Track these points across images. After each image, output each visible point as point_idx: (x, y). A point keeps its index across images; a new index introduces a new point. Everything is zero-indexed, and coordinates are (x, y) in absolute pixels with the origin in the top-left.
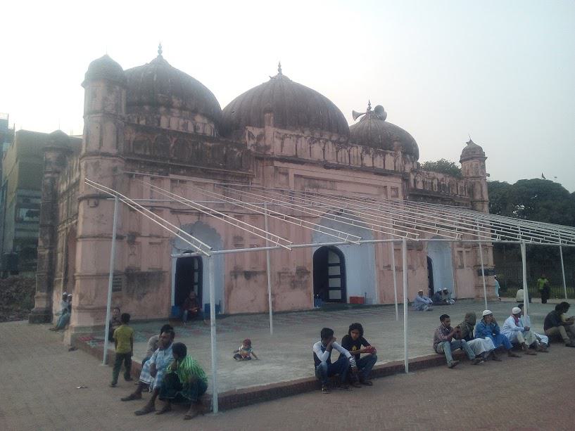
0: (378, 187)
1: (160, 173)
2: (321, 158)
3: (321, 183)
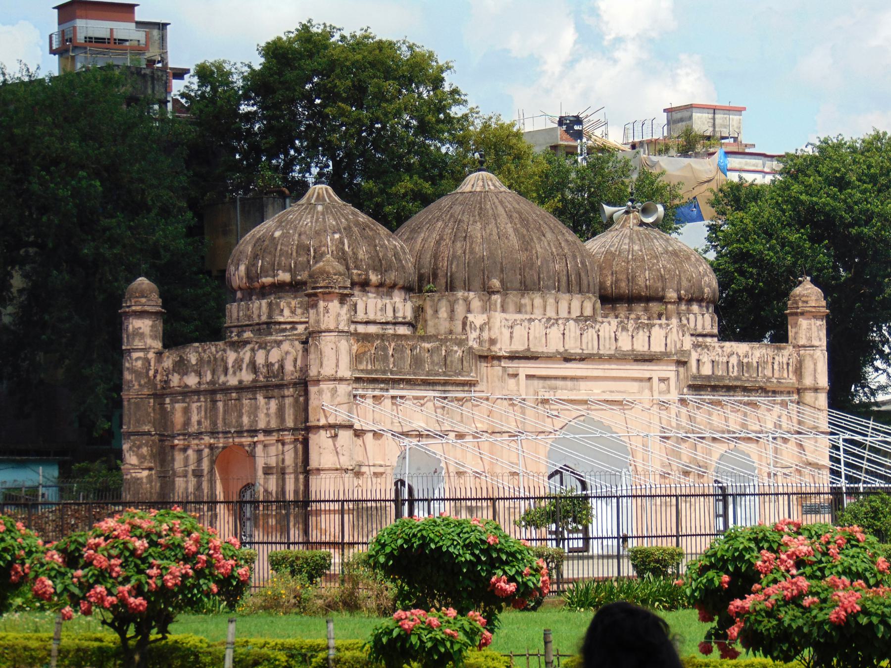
0: (641, 380)
1: (381, 389)
2: (561, 350)
3: (560, 383)
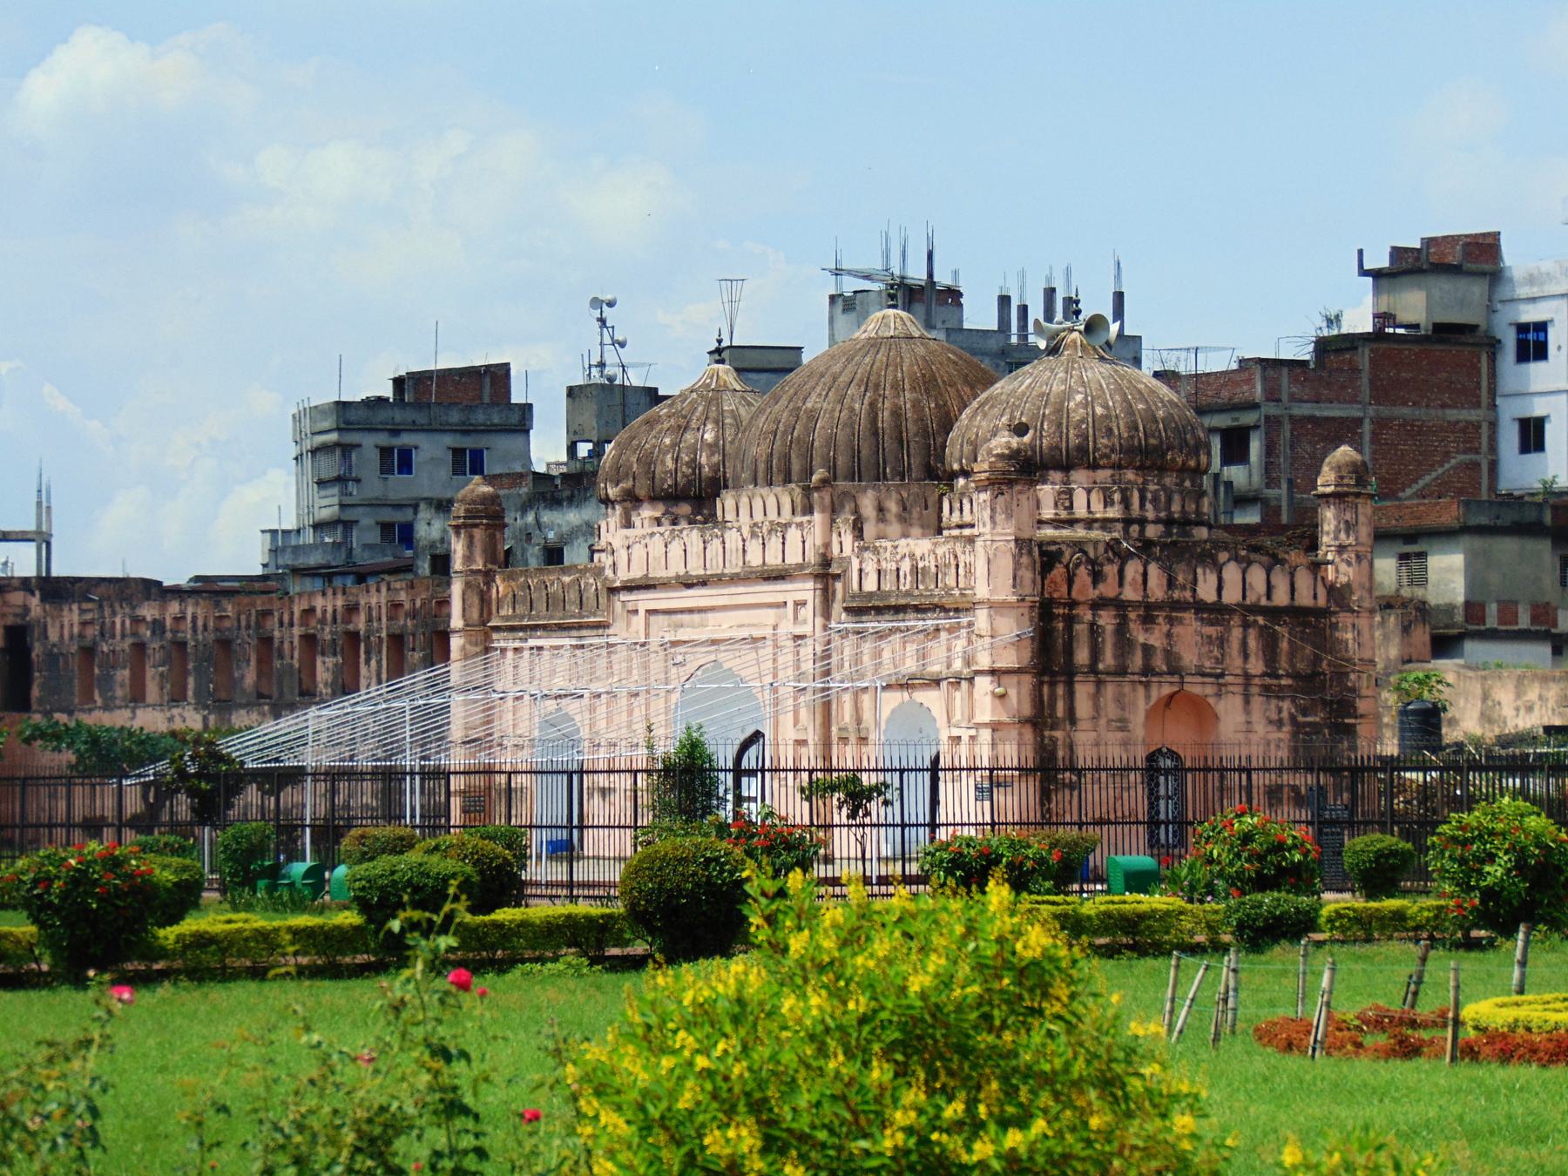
2: (682, 572)
3: (686, 618)
